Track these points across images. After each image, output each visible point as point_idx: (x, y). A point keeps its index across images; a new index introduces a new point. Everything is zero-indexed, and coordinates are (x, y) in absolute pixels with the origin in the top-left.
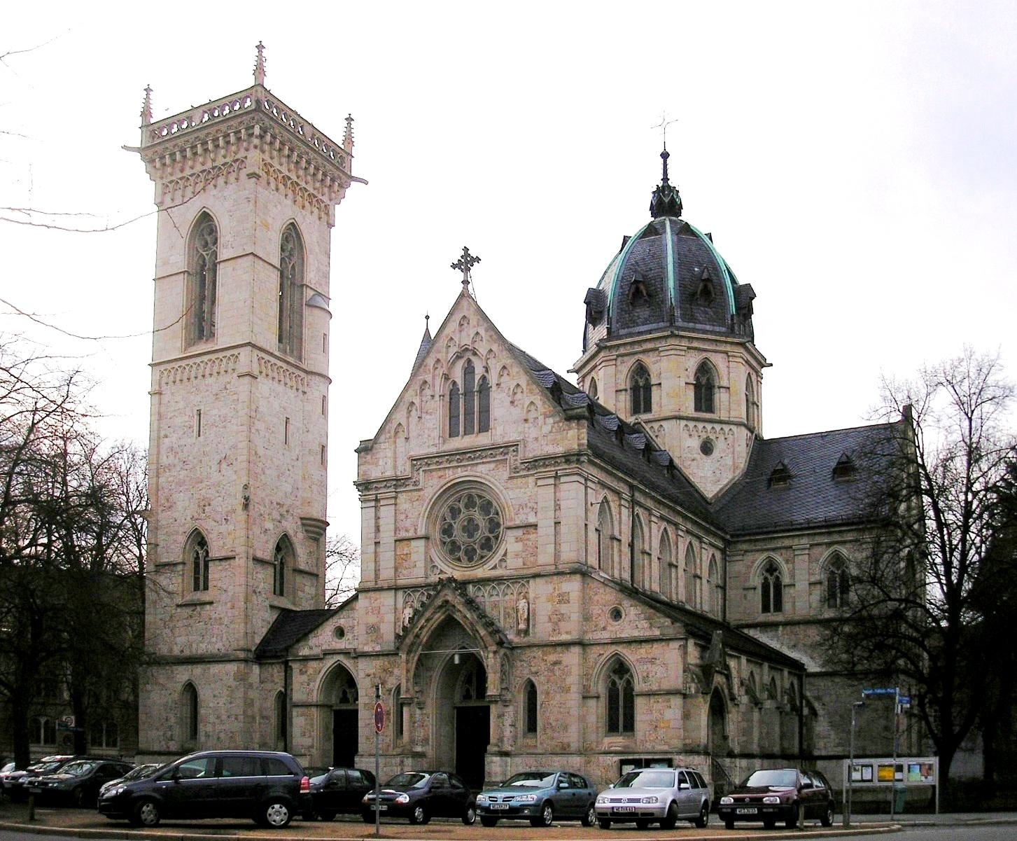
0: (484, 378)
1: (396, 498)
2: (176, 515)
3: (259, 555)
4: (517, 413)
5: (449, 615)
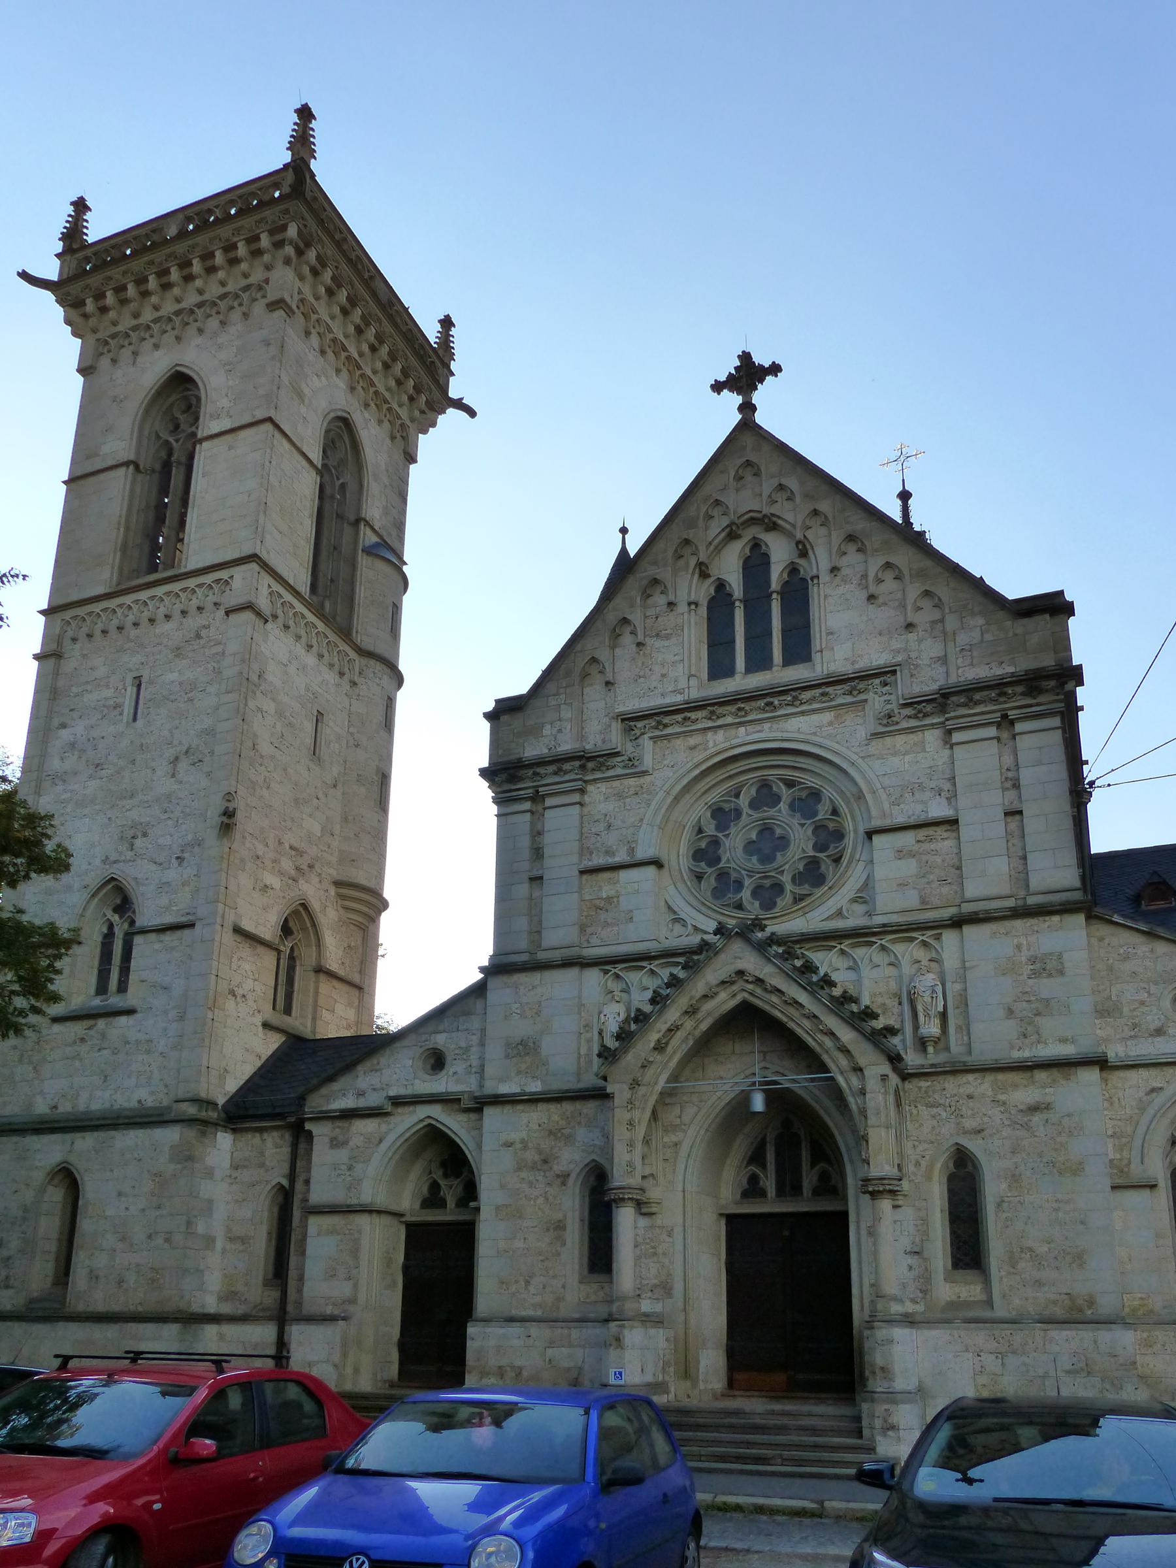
1: (582, 791)
3: (248, 925)
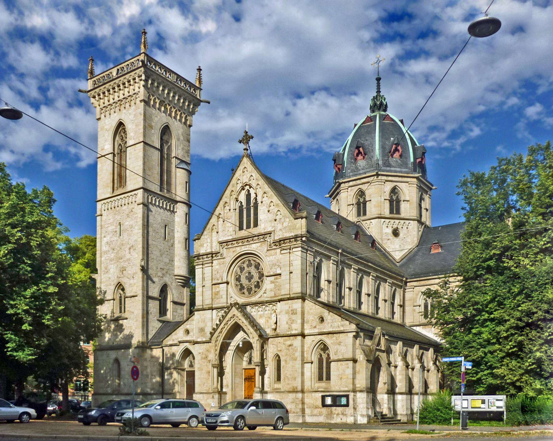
0: (256, 199)
1: (212, 263)
2: (110, 276)
4: (271, 216)
5: (236, 322)
